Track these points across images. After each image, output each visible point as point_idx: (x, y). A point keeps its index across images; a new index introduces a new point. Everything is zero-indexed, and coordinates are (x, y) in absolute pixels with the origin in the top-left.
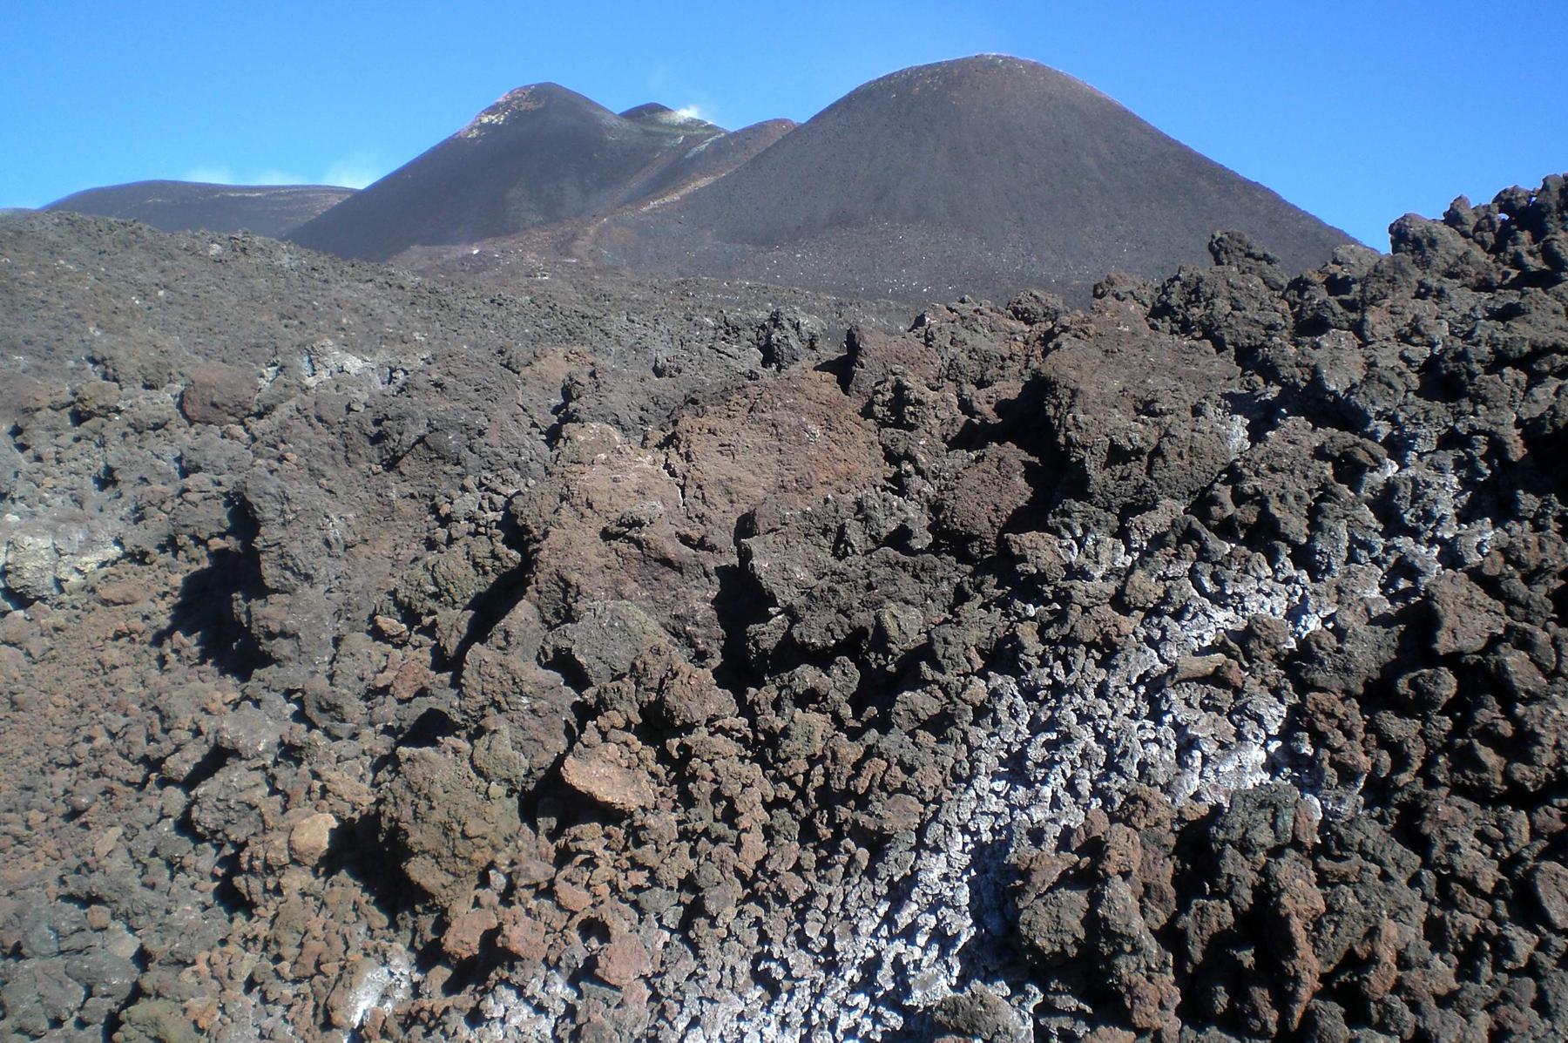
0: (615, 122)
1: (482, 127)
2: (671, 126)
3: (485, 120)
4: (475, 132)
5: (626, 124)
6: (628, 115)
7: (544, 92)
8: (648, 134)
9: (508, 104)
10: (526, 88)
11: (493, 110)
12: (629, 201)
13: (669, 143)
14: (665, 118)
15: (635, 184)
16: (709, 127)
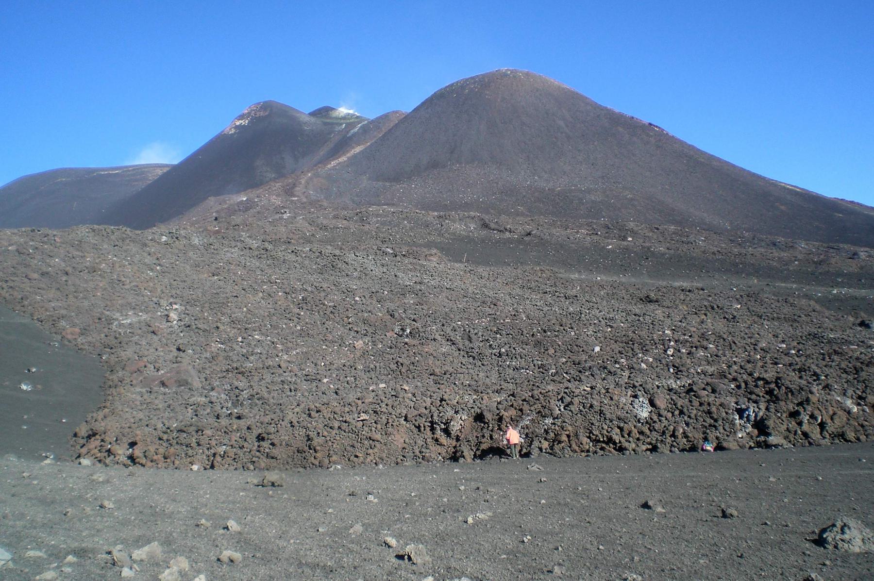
0: (307, 119)
1: (236, 127)
2: (337, 118)
3: (238, 123)
4: (233, 131)
5: (313, 119)
6: (313, 114)
7: (267, 106)
8: (325, 124)
9: (249, 113)
10: (259, 104)
11: (241, 117)
12: (320, 163)
13: (337, 129)
14: (335, 114)
15: (322, 152)
16: (358, 117)
